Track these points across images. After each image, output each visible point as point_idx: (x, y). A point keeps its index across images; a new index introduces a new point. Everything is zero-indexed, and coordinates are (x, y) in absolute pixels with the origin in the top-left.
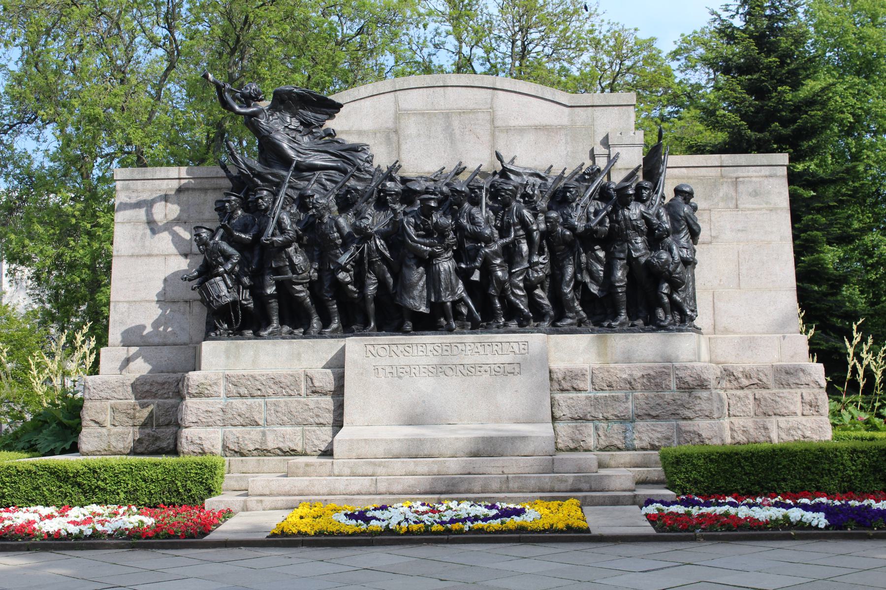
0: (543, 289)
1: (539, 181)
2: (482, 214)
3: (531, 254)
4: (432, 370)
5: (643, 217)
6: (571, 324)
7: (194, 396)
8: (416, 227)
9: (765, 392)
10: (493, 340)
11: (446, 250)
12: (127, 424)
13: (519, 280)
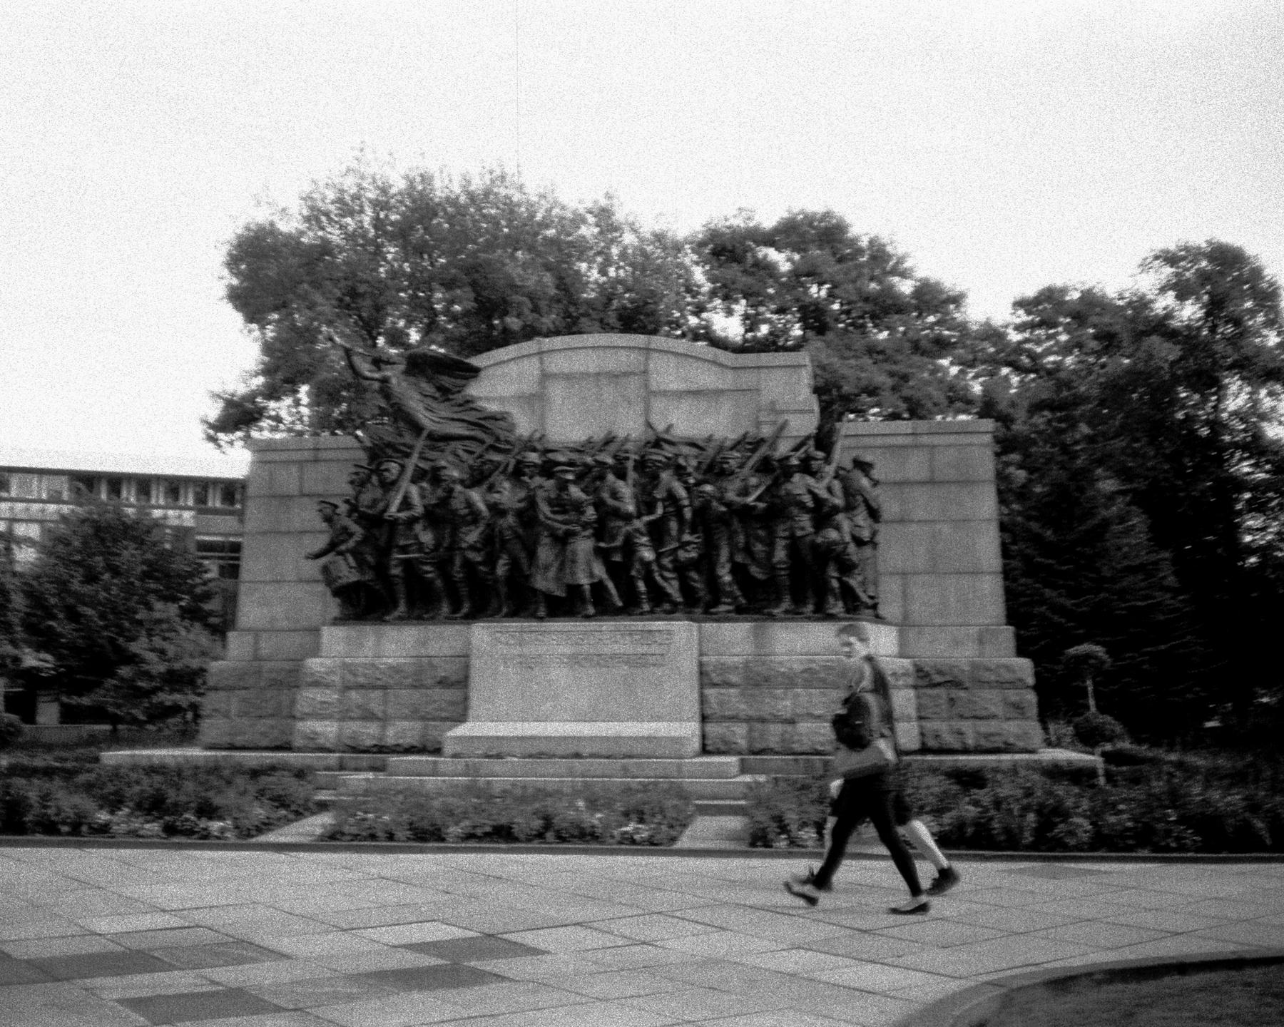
0: (699, 572)
1: (694, 451)
2: (626, 490)
3: (681, 531)
5: (810, 492)
6: (729, 612)
8: (550, 502)
9: (962, 694)
13: (666, 561)
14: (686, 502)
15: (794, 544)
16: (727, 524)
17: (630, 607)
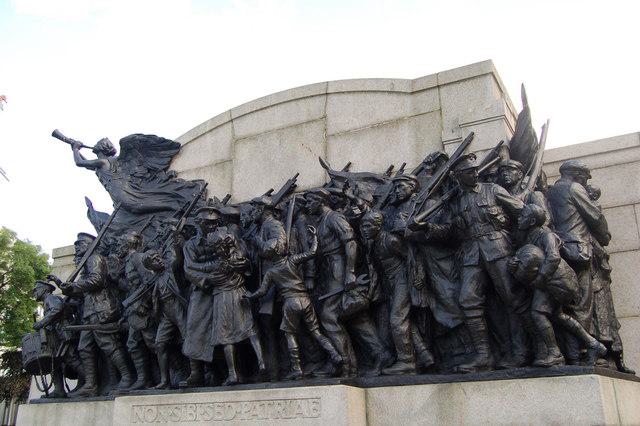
1: (373, 186)
5: (499, 202)
6: (407, 371)
10: (275, 397)
11: (230, 273)
13: (330, 312)
14: (350, 235)
15: (485, 269)
16: (403, 259)
17: (280, 375)
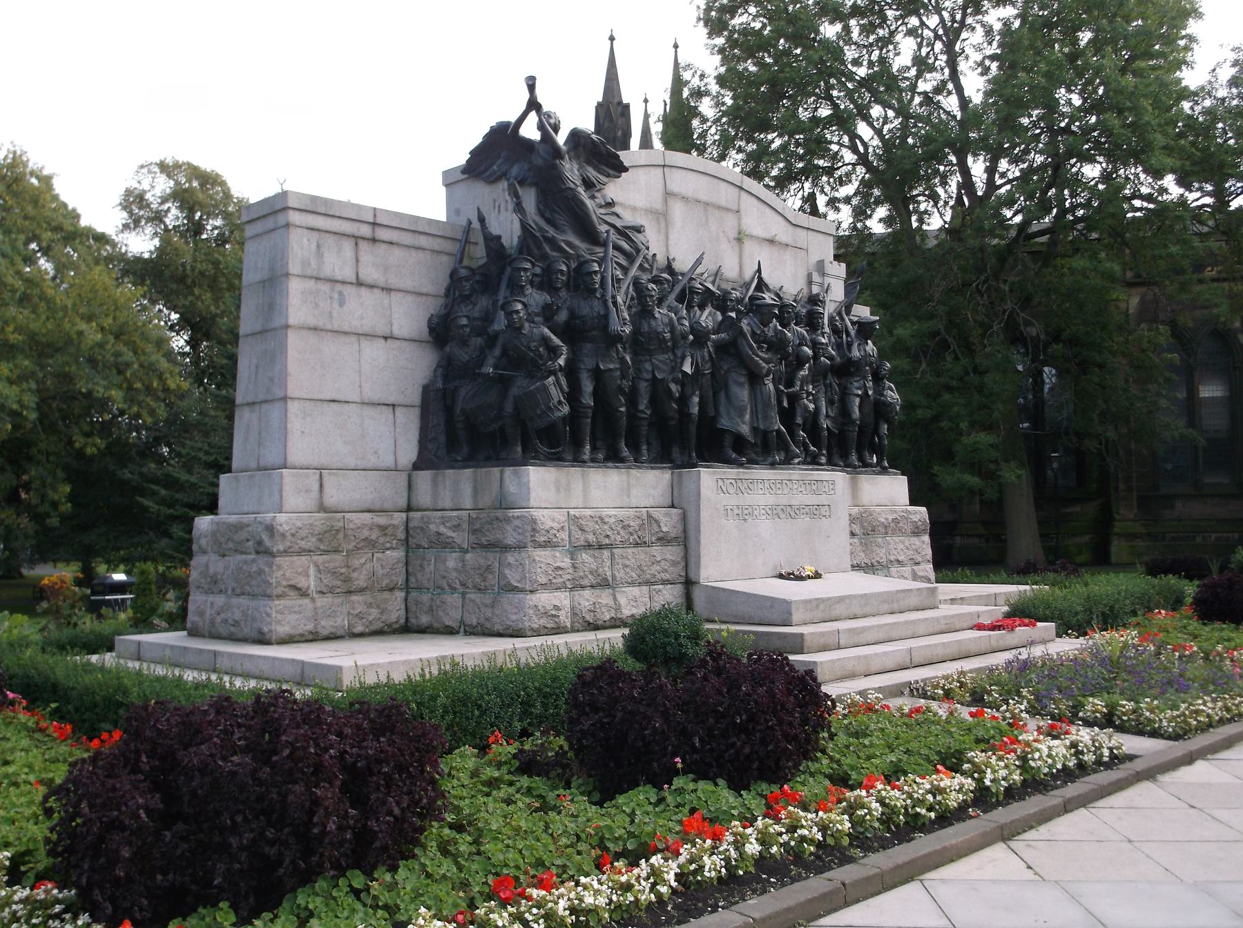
4: (769, 512)
7: (541, 546)
12: (339, 590)
